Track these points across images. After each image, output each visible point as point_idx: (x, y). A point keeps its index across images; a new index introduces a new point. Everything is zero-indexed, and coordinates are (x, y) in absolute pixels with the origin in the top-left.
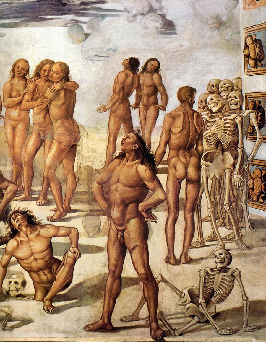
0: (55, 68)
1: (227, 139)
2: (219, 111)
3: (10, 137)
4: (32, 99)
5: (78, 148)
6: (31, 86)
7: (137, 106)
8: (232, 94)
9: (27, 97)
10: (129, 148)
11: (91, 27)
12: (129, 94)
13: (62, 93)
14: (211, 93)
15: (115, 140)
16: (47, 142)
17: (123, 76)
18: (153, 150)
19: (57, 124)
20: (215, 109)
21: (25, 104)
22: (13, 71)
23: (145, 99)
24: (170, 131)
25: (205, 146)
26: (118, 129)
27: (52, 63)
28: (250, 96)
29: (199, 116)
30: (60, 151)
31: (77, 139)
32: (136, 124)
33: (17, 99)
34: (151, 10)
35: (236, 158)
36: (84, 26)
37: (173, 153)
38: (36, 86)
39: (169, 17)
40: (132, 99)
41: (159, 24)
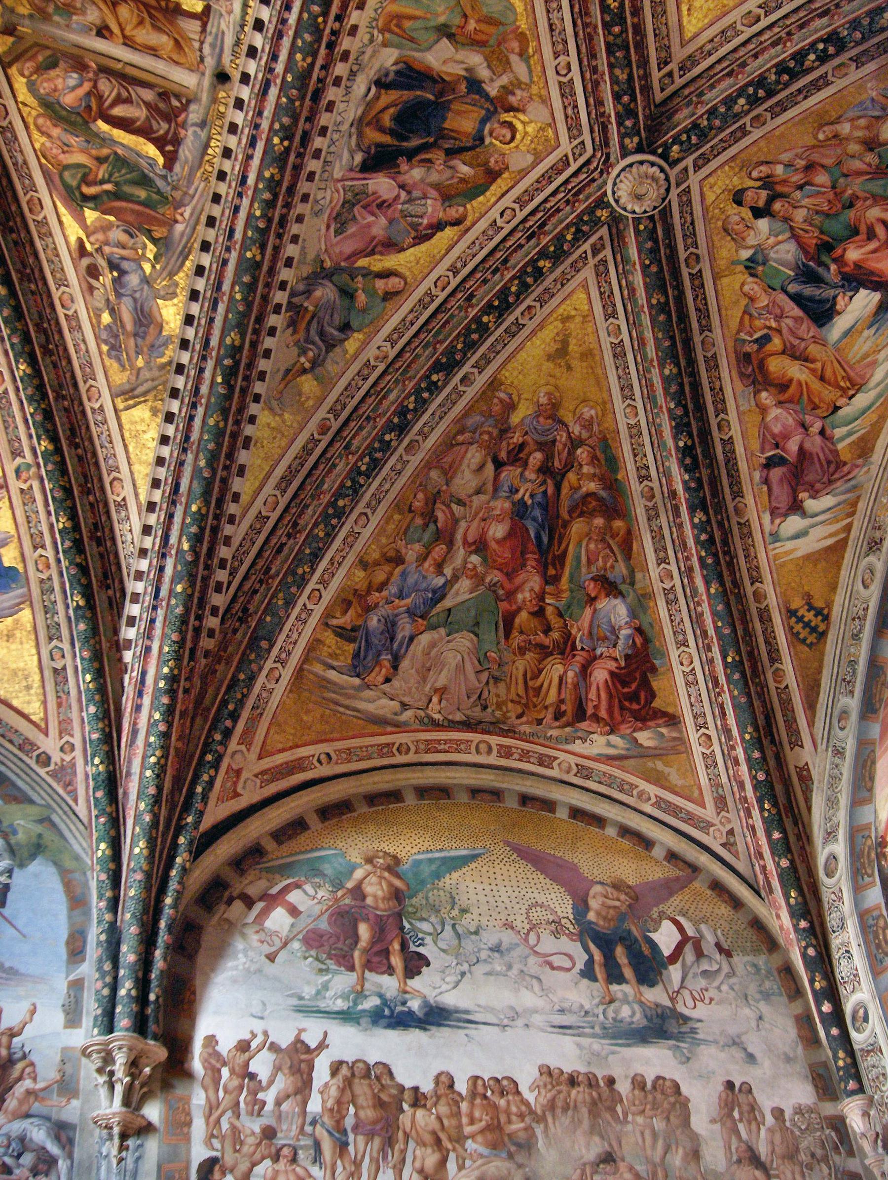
0: (668, 1083)
1: (819, 1152)
2: (807, 1129)
3: (640, 1141)
4: (653, 1109)
5: (701, 1153)
6: (650, 1097)
7: (741, 1120)
8: (813, 1115)
9: (648, 1106)
10: (742, 1155)
11: (690, 1051)
12: (733, 1110)
13: (678, 1106)
14: (796, 1113)
15: (730, 1148)
16: (674, 1147)
17: (724, 1095)
18: (763, 1158)
19: (678, 1132)
20: (803, 1127)
21: (648, 1112)
22: (633, 1082)
23: (746, 1115)
24: (772, 1143)
25: (804, 1157)
26: (730, 1138)
27: (664, 1079)
28: (826, 1118)
29: (792, 1132)
30: (686, 1155)
31: (699, 1145)
32: (744, 1135)
33: (641, 1108)
34: (734, 1043)
35: (830, 1168)
36: (685, 1051)
37: (780, 1161)
38: (655, 1098)
39: (750, 1050)
40: (736, 1114)
41: (743, 1055)
